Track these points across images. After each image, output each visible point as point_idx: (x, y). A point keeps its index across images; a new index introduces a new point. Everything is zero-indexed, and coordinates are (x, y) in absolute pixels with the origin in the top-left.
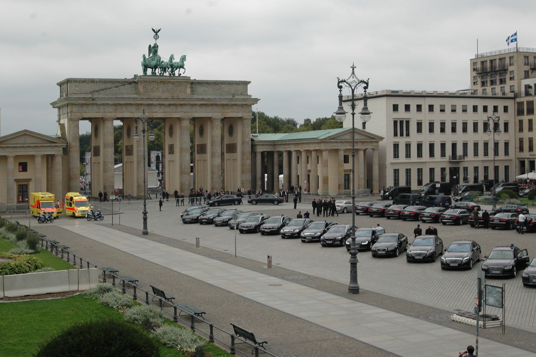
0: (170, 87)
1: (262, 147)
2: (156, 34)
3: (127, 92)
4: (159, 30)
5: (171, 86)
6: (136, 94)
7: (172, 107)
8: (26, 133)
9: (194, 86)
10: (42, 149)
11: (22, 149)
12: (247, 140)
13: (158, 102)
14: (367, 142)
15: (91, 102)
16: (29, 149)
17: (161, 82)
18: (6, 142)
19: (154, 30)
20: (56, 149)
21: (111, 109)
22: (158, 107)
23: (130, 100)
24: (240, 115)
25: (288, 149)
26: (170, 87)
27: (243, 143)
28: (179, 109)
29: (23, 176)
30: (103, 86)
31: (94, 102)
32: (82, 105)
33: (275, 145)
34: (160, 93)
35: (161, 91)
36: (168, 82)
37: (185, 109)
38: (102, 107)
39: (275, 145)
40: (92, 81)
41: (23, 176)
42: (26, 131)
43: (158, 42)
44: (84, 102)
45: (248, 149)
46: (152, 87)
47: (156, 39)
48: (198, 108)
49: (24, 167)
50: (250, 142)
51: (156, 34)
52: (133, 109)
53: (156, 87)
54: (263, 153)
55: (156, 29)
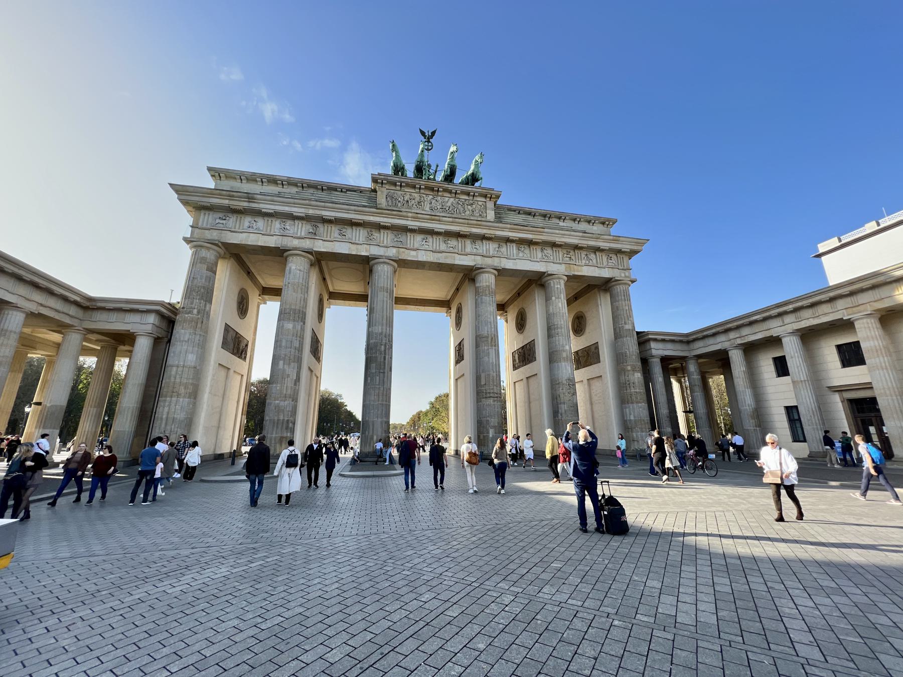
2: (429, 142)
4: (433, 133)
7: (453, 242)
19: (423, 133)
21: (302, 229)
24: (606, 273)
27: (618, 334)
28: (469, 246)
33: (688, 342)
38: (277, 224)
44: (226, 202)
45: (631, 347)
48: (513, 249)
52: (360, 234)
53: (418, 199)
55: (428, 131)
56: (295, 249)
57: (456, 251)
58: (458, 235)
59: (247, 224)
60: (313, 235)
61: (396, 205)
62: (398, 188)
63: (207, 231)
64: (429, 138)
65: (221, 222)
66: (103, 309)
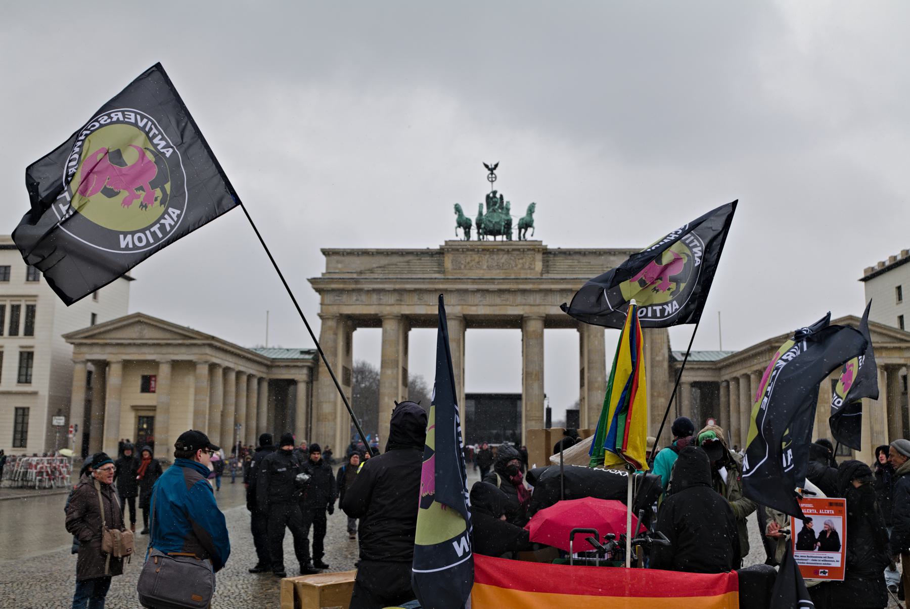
0: (503, 261)
1: (692, 373)
2: (492, 174)
3: (426, 271)
4: (496, 166)
5: (503, 258)
6: (439, 272)
7: (506, 296)
8: (142, 319)
9: (551, 257)
10: (170, 350)
11: (134, 350)
12: (657, 359)
13: (475, 287)
14: (886, 348)
15: (353, 286)
16: (145, 350)
17: (484, 250)
18: (108, 336)
19: (487, 166)
20: (195, 350)
21: (392, 299)
22: (479, 295)
25: (735, 375)
26: (503, 261)
28: (519, 299)
29: (147, 399)
30: (384, 261)
31: (359, 286)
32: (341, 291)
34: (484, 269)
35: (485, 267)
36: (498, 250)
37: (531, 299)
38: (375, 297)
39: (720, 369)
40: (365, 253)
41: (147, 399)
42: (139, 315)
43: (500, 188)
44: (341, 286)
46: (468, 259)
47: (492, 181)
49: (147, 386)
50: (666, 365)
51: (492, 174)
53: (477, 260)
54: (694, 384)
55: (491, 164)
56: (389, 315)
58: (508, 291)
59: (355, 298)
60: (400, 302)
61: (460, 268)
64: (492, 170)
66: (278, 366)
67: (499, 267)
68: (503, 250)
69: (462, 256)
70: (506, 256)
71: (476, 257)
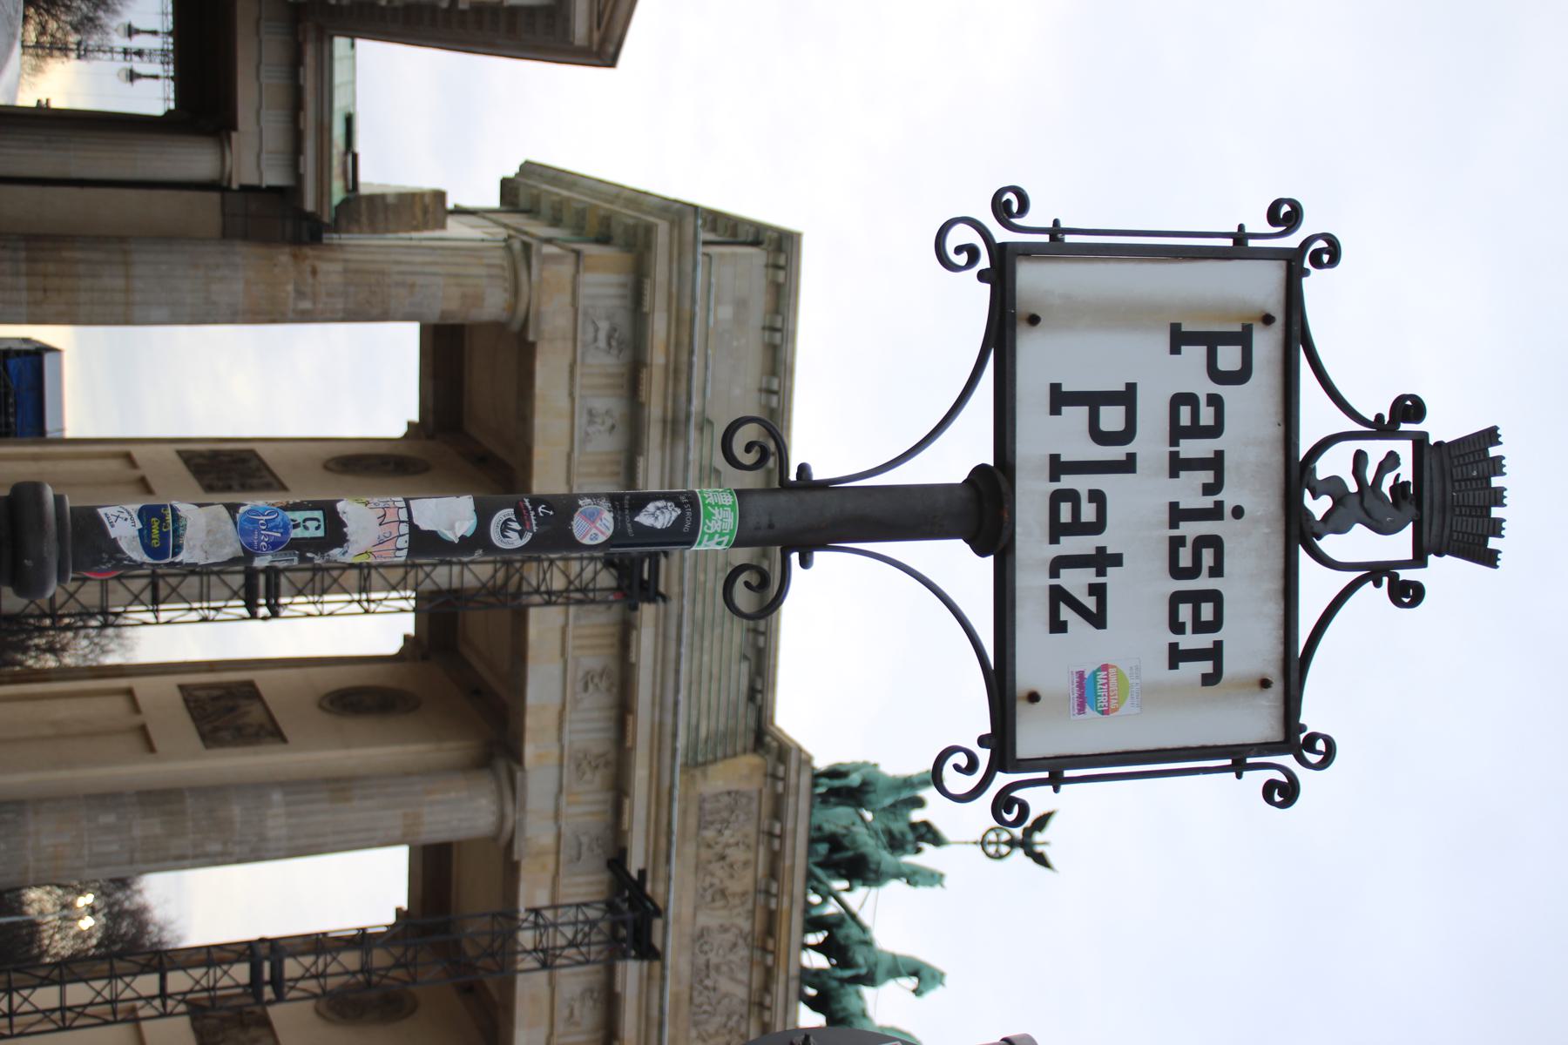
4: (1041, 859)
5: (735, 988)
6: (693, 747)
15: (655, 410)
23: (659, 702)
26: (725, 985)
31: (654, 435)
35: (703, 920)
44: (657, 357)
47: (983, 843)
52: (589, 727)
53: (734, 886)
57: (560, 1027)
61: (702, 825)
62: (765, 825)
63: (567, 299)
65: (602, 336)
67: (703, 972)
68: (766, 988)
69: (751, 829)
70: (741, 992)
71: (744, 882)
